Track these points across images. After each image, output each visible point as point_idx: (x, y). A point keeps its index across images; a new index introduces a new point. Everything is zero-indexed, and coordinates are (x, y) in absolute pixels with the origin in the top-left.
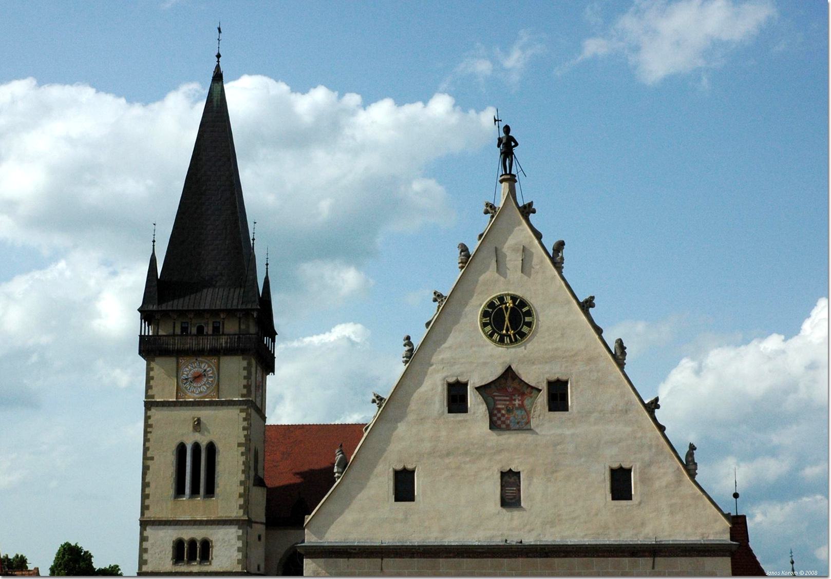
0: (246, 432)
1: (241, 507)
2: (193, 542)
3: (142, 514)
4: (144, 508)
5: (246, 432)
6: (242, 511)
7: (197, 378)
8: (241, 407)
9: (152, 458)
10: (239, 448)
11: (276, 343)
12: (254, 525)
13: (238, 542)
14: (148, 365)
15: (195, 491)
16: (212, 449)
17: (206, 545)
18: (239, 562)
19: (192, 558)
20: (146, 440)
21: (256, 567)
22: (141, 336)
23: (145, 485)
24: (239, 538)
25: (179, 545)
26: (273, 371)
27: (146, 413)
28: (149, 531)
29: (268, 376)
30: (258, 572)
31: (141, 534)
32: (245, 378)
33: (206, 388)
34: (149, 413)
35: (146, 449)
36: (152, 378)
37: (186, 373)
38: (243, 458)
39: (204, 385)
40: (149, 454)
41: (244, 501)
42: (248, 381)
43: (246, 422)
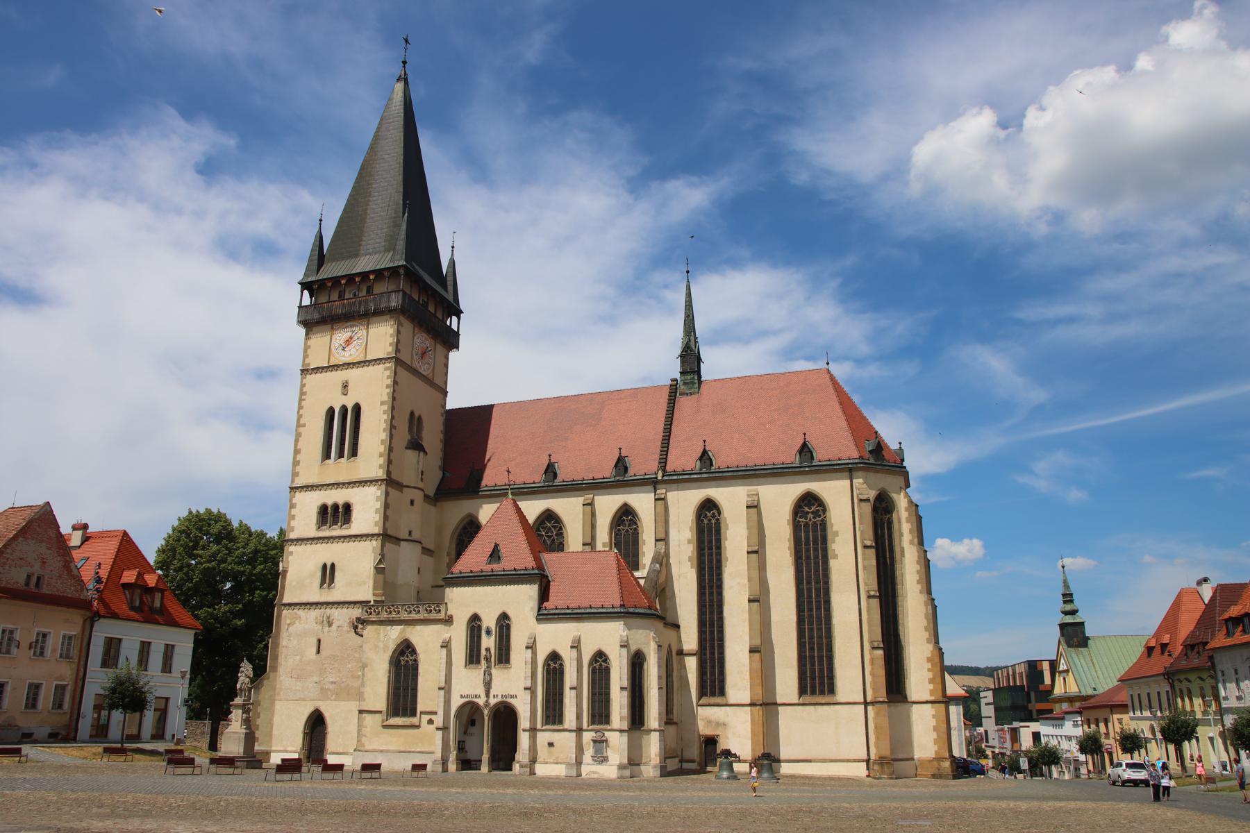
0: (388, 390)
1: (380, 467)
2: (336, 506)
3: (293, 481)
4: (295, 475)
5: (388, 390)
6: (382, 470)
7: (349, 342)
8: (387, 365)
9: (304, 425)
10: (382, 407)
11: (461, 321)
12: (405, 489)
13: (376, 503)
14: (307, 334)
15: (341, 455)
16: (357, 409)
17: (348, 508)
18: (376, 524)
19: (335, 522)
20: (300, 407)
21: (408, 533)
22: (300, 307)
23: (297, 452)
24: (378, 499)
25: (323, 510)
26: (457, 347)
27: (302, 381)
28: (299, 496)
29: (450, 353)
30: (410, 538)
31: (291, 500)
32: (391, 335)
33: (355, 350)
34: (304, 381)
35: (300, 416)
36: (309, 347)
37: (338, 338)
38: (385, 417)
39: (354, 347)
40: (302, 421)
41: (384, 460)
42: (394, 339)
43: (390, 380)
